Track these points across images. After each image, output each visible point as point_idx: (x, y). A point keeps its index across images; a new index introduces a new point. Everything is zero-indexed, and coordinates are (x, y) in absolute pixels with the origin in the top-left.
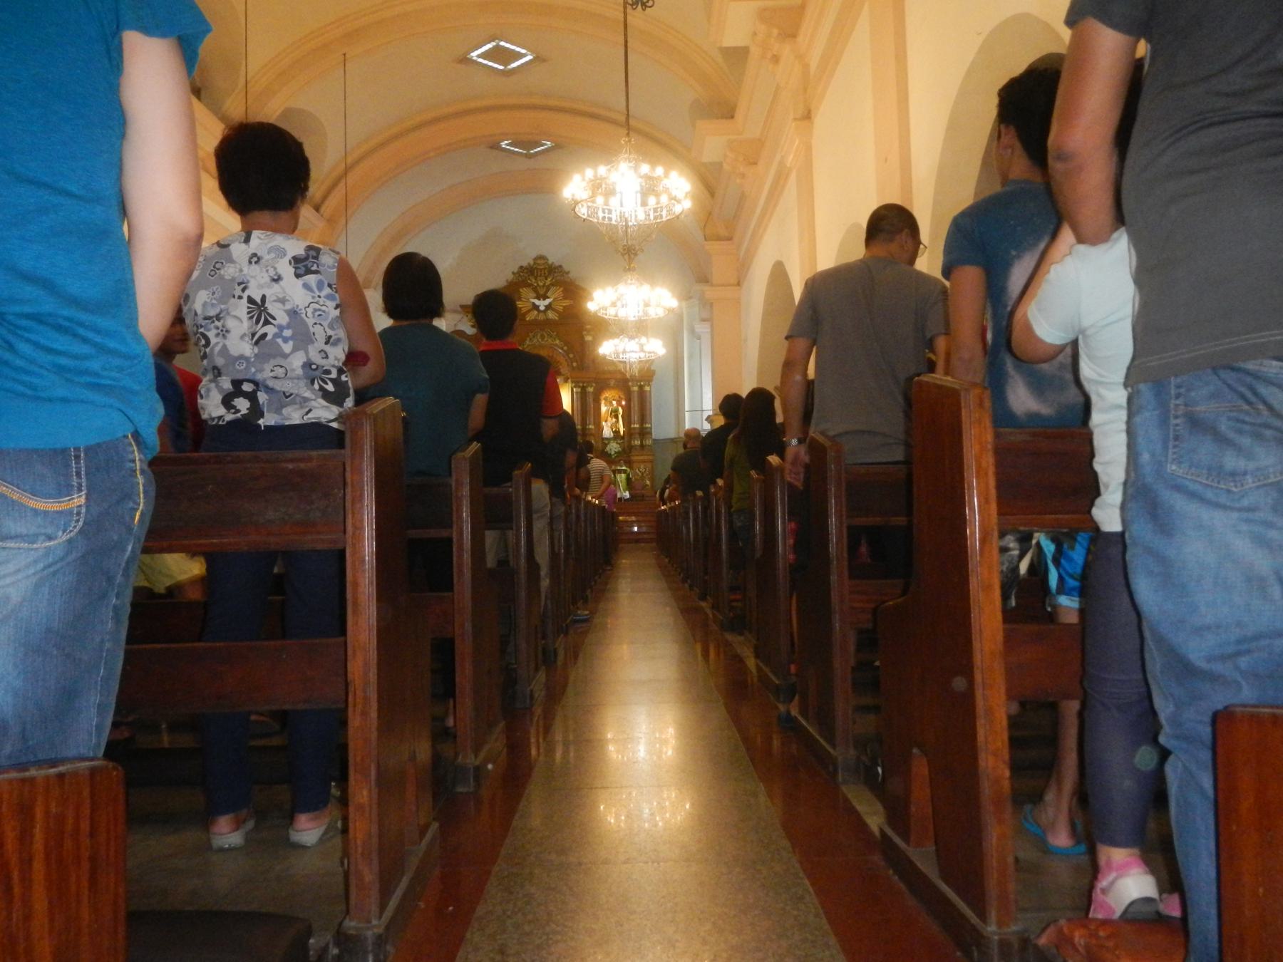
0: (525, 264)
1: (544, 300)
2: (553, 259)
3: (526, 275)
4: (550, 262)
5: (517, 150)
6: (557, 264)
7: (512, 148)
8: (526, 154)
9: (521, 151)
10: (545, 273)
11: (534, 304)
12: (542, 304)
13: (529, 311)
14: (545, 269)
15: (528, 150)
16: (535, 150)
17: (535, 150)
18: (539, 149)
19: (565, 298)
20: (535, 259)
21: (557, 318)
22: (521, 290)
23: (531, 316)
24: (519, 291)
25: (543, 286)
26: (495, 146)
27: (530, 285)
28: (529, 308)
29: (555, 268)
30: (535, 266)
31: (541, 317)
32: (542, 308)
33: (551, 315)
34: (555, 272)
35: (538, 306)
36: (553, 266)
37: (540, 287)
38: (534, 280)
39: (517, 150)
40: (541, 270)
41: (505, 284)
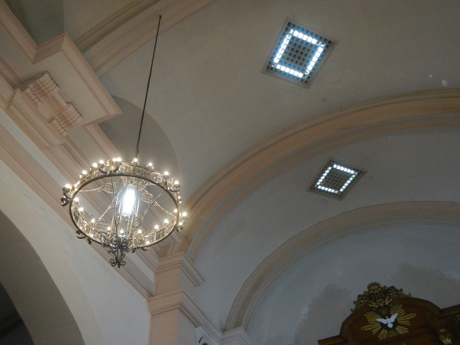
0: (362, 293)
1: (389, 317)
2: (385, 283)
3: (367, 301)
4: (382, 286)
5: (330, 190)
6: (389, 286)
7: (326, 189)
8: (337, 195)
9: (333, 191)
10: (381, 296)
11: (381, 323)
12: (389, 322)
13: (380, 331)
14: (380, 291)
15: (338, 189)
16: (344, 187)
17: (344, 187)
18: (346, 184)
19: (407, 313)
20: (369, 287)
21: (407, 332)
22: (366, 315)
23: (384, 334)
24: (367, 317)
25: (385, 306)
26: (313, 188)
27: (371, 309)
28: (380, 327)
29: (389, 289)
30: (371, 292)
31: (393, 334)
32: (390, 326)
33: (401, 330)
34: (390, 293)
35: (387, 325)
36: (386, 288)
37: (380, 307)
38: (374, 304)
39: (330, 190)
40: (377, 294)
41: (350, 313)
